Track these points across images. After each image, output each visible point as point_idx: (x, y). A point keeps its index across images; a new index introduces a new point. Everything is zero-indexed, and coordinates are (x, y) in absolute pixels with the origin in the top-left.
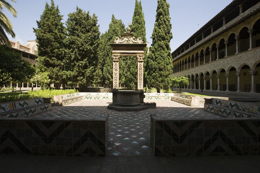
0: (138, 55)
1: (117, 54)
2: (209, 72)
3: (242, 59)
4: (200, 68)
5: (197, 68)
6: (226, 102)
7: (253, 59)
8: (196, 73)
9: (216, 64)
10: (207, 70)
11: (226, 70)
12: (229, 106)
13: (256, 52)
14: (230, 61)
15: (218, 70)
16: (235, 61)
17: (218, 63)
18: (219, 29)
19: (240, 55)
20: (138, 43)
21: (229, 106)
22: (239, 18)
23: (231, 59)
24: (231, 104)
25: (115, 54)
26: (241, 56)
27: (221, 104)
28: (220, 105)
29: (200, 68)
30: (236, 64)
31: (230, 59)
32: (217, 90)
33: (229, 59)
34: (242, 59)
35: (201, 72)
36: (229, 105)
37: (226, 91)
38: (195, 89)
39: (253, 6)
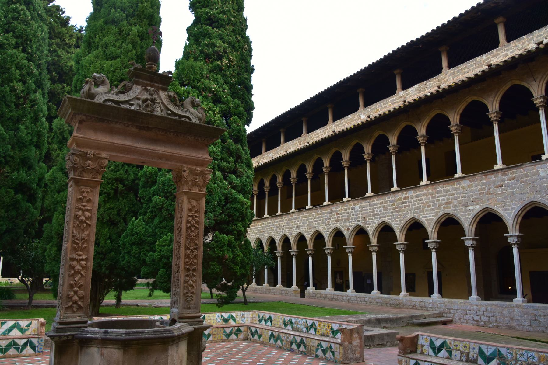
0: (186, 167)
1: (97, 152)
2: (324, 235)
3: (409, 206)
4: (295, 218)
5: (286, 218)
6: (465, 347)
7: (433, 210)
8: (282, 233)
9: (344, 213)
10: (317, 228)
11: (370, 233)
12: (477, 357)
13: (438, 192)
14: (380, 207)
15: (348, 229)
16: (393, 209)
17: (349, 209)
18: (349, 116)
19: (404, 196)
20: (187, 120)
21: (477, 357)
22: (396, 99)
23: (381, 203)
24: (481, 353)
25: (84, 150)
26: (405, 198)
27: (450, 352)
28: (447, 355)
29: (295, 218)
30: (395, 219)
31: (379, 202)
32: (349, 291)
33: (375, 202)
34: (409, 206)
35: (298, 231)
36: (475, 356)
37: (348, 291)
38: (266, 285)
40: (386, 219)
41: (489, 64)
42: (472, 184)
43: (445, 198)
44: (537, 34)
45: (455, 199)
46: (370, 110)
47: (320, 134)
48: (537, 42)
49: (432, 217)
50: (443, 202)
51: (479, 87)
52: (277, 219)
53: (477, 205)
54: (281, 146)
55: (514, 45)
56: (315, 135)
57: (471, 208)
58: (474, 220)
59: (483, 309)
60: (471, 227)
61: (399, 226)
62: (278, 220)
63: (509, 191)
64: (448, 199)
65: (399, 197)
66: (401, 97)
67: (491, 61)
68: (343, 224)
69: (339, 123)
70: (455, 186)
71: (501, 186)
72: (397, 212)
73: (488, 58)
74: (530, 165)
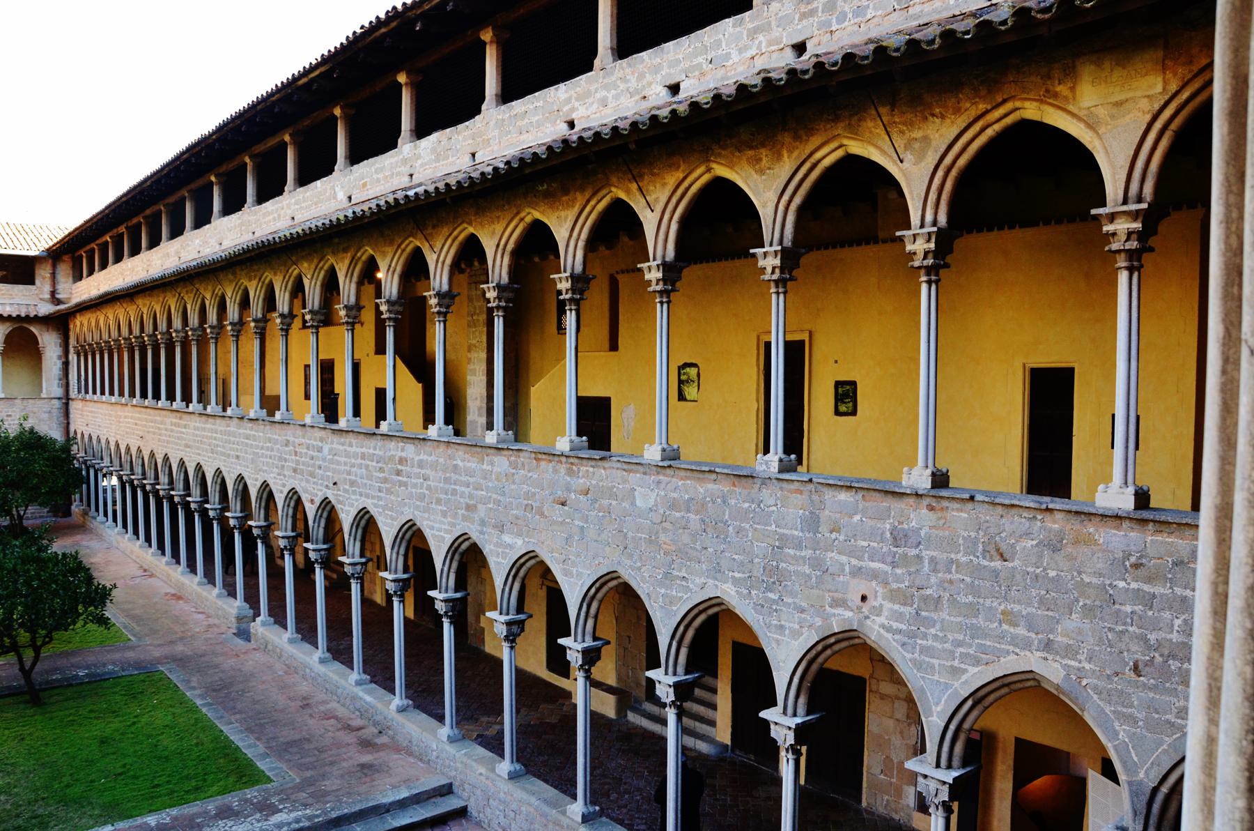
3: (405, 484)
14: (360, 466)
23: (363, 457)
31: (359, 450)
39: (448, 130)
40: (370, 501)
41: (569, 119)
42: (513, 474)
43: (467, 490)
44: (671, 57)
45: (485, 501)
46: (352, 177)
47: (271, 217)
48: (667, 84)
49: (442, 534)
50: (462, 500)
51: (545, 187)
52: (206, 422)
53: (519, 535)
54: (162, 244)
55: (621, 74)
56: (265, 215)
57: (507, 538)
58: (512, 573)
59: (514, 806)
60: (507, 589)
61: (390, 531)
62: (208, 426)
63: (576, 522)
64: (471, 496)
65: (393, 453)
66: (405, 161)
67: (573, 110)
68: (303, 484)
69: (301, 197)
70: (485, 467)
71: (563, 504)
72: (389, 492)
73: (568, 100)
74: (619, 465)
